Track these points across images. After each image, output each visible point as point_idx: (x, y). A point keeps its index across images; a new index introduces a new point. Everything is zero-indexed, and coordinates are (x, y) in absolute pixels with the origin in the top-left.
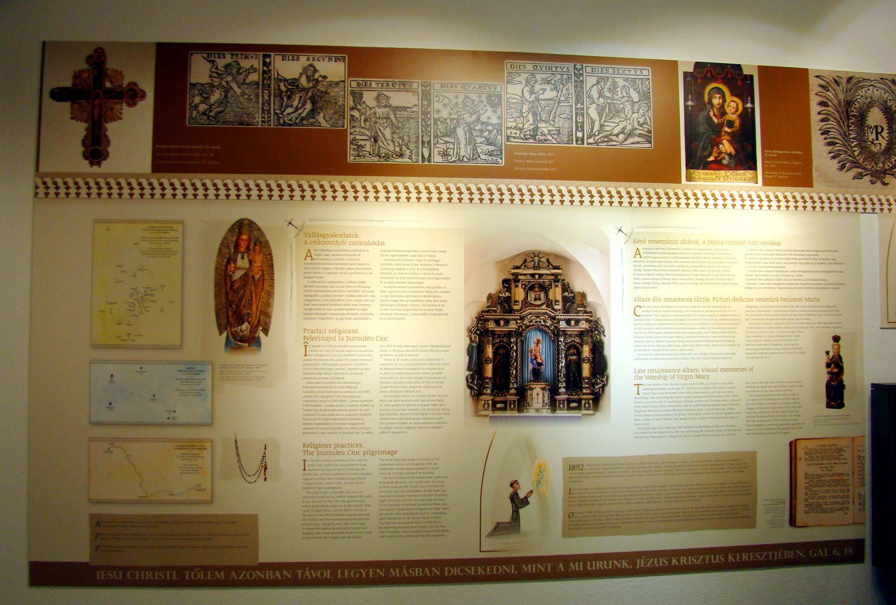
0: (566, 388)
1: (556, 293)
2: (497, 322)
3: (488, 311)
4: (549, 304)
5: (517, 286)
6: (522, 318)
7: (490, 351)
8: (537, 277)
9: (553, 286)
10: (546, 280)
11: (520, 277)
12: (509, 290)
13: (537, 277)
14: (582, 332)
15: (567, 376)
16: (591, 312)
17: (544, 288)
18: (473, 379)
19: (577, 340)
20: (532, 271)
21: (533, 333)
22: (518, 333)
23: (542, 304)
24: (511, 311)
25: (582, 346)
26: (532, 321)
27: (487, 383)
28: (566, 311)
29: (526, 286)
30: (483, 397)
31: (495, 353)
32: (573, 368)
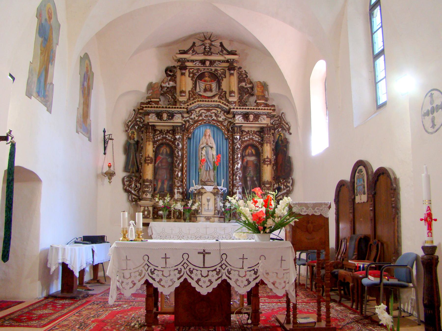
1: (231, 83)
2: (159, 115)
3: (149, 103)
4: (222, 95)
5: (183, 74)
6: (189, 112)
7: (150, 150)
8: (208, 63)
10: (219, 68)
12: (173, 78)
13: (208, 63)
14: (262, 128)
16: (273, 106)
17: (216, 78)
18: (130, 182)
19: (256, 138)
20: (201, 57)
21: (202, 129)
22: (184, 129)
23: (214, 96)
24: (175, 102)
25: (262, 145)
26: (201, 115)
27: (147, 186)
28: (242, 103)
29: (194, 74)
30: (142, 202)
31: (156, 152)
32: (251, 172)
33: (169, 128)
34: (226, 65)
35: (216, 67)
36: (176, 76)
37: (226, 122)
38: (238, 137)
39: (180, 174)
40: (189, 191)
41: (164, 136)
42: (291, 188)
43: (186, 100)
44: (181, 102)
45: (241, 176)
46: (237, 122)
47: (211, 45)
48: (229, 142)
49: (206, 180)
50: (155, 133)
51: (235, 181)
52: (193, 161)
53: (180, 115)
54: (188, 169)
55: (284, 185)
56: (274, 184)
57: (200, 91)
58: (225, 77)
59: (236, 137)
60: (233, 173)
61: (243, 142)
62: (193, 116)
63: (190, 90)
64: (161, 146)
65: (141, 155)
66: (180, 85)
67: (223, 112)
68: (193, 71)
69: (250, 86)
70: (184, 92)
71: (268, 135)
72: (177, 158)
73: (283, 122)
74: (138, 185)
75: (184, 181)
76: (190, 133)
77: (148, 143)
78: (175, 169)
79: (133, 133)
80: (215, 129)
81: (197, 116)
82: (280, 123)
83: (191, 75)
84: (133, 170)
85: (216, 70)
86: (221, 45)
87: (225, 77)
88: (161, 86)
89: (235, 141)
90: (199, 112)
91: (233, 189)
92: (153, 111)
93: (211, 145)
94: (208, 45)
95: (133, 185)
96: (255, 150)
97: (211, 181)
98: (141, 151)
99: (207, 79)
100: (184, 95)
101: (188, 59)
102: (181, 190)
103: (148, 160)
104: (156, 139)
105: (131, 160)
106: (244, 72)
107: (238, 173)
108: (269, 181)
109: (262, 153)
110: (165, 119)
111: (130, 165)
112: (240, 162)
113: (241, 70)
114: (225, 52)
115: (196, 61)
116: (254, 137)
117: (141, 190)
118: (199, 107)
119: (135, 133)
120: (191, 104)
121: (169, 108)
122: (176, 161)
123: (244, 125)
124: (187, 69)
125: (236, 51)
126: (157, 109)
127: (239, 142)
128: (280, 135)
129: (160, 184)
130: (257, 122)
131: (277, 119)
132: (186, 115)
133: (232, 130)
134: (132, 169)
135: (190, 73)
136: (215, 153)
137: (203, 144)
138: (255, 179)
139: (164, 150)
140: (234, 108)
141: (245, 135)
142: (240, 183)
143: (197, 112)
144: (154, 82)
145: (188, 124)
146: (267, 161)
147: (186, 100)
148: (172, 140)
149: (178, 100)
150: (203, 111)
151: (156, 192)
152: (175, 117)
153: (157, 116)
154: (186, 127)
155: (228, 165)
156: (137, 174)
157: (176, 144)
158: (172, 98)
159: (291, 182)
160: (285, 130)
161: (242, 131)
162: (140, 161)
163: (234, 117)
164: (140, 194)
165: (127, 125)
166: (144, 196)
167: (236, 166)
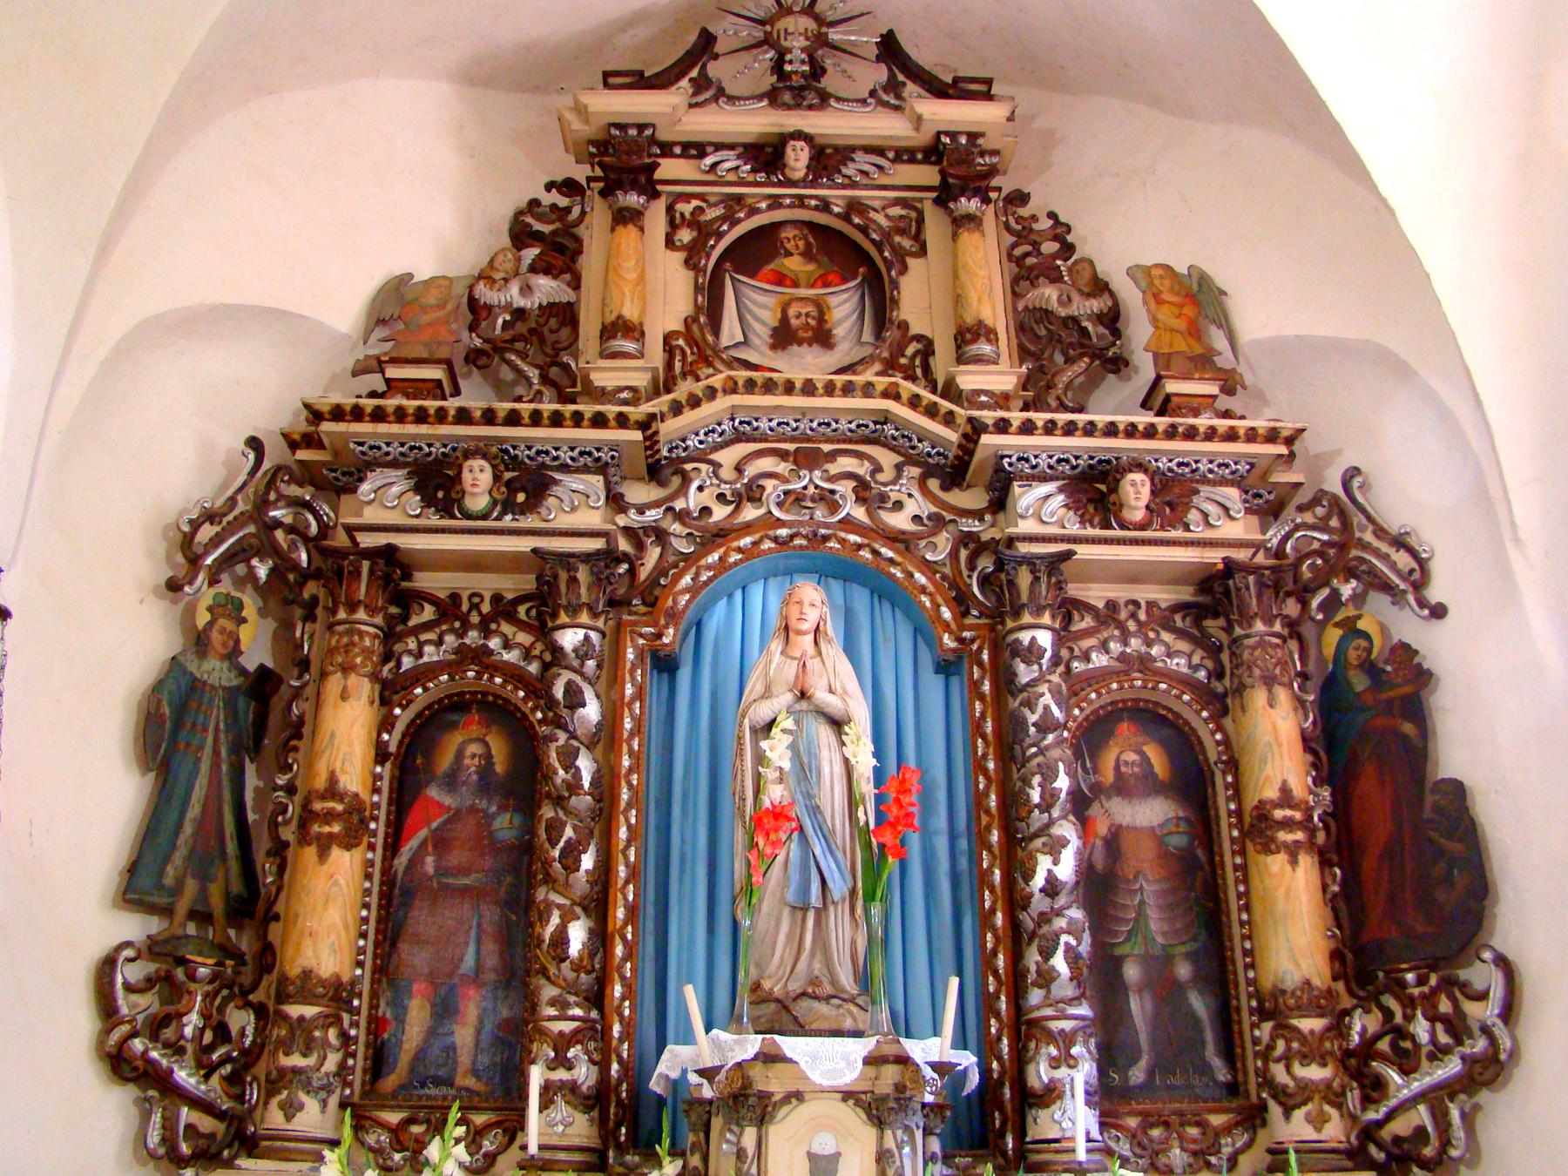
0: (1109, 1098)
2: (436, 482)
4: (907, 356)
5: (626, 217)
7: (347, 737)
8: (798, 158)
9: (935, 226)
10: (880, 194)
11: (670, 168)
13: (798, 158)
15: (1102, 975)
19: (1176, 656)
20: (755, 122)
21: (763, 598)
22: (623, 584)
26: (752, 493)
31: (407, 765)
33: (511, 585)
34: (928, 175)
35: (854, 185)
36: (578, 241)
37: (944, 541)
38: (1045, 639)
39: (578, 935)
40: (656, 1085)
41: (473, 638)
42: (1505, 1043)
43: (641, 380)
44: (603, 395)
45: (1084, 948)
46: (1027, 526)
47: (821, 41)
48: (975, 686)
49: (795, 986)
50: (405, 618)
51: (1035, 996)
52: (690, 834)
53: (597, 481)
54: (651, 895)
55: (1433, 1018)
56: (1347, 1013)
57: (746, 343)
58: (922, 251)
59: (1025, 637)
60: (1014, 925)
61: (1075, 688)
62: (693, 500)
63: (677, 326)
64: (455, 717)
65: (281, 780)
66: (606, 283)
67: (915, 471)
68: (700, 210)
69: (1095, 305)
70: (633, 331)
71: (1269, 621)
72: (559, 801)
73: (1368, 537)
74: (241, 1020)
75: (618, 990)
76: (673, 616)
77: (335, 683)
78: (541, 894)
79: (230, 609)
80: (861, 599)
81: (721, 497)
82: (1345, 540)
83: (685, 236)
84: (203, 893)
85: (855, 207)
86: (890, 49)
88: (473, 303)
89: (1025, 673)
90: (739, 469)
91: (1021, 1059)
92: (396, 450)
93: (833, 703)
94: (797, 44)
95: (193, 1021)
96: (1165, 745)
97: (836, 996)
98: (287, 748)
99: (794, 264)
100: (629, 346)
101: (664, 135)
102: (584, 1073)
103: (329, 817)
104: (407, 662)
105: (194, 810)
106: (1045, 224)
107: (1061, 923)
108: (1316, 982)
109: (1233, 765)
110: (478, 501)
111: (179, 857)
112: (1067, 830)
113: (1024, 212)
114: (911, 88)
115: (719, 147)
116: (1155, 651)
117: (260, 1069)
118: (739, 438)
119: (250, 611)
120: (677, 409)
121: (513, 419)
122: (554, 829)
123: (1083, 551)
124: (655, 195)
125: (989, 82)
126: (424, 429)
127: (1055, 678)
128: (1351, 629)
129: (418, 1015)
130: (1178, 533)
131: (1308, 518)
132: (637, 493)
133: (996, 588)
134: (191, 886)
135: (673, 226)
136: (865, 762)
137: (767, 694)
138: (1183, 971)
139: (471, 747)
140: (1002, 427)
141: (1087, 633)
142: (1084, 1010)
143: (727, 473)
144: (423, 273)
145: (653, 554)
146: (1288, 824)
147: (641, 380)
148: (534, 668)
149: (587, 381)
150: (767, 464)
151: (390, 1082)
152: (556, 490)
153: (417, 489)
155: (963, 863)
156: (245, 942)
157: (559, 692)
158: (545, 379)
159: (1497, 993)
160: (1386, 587)
161: (1068, 609)
162: (274, 826)
163: (999, 503)
164: (253, 1094)
165: (187, 541)
166: (275, 1118)
167: (1044, 863)
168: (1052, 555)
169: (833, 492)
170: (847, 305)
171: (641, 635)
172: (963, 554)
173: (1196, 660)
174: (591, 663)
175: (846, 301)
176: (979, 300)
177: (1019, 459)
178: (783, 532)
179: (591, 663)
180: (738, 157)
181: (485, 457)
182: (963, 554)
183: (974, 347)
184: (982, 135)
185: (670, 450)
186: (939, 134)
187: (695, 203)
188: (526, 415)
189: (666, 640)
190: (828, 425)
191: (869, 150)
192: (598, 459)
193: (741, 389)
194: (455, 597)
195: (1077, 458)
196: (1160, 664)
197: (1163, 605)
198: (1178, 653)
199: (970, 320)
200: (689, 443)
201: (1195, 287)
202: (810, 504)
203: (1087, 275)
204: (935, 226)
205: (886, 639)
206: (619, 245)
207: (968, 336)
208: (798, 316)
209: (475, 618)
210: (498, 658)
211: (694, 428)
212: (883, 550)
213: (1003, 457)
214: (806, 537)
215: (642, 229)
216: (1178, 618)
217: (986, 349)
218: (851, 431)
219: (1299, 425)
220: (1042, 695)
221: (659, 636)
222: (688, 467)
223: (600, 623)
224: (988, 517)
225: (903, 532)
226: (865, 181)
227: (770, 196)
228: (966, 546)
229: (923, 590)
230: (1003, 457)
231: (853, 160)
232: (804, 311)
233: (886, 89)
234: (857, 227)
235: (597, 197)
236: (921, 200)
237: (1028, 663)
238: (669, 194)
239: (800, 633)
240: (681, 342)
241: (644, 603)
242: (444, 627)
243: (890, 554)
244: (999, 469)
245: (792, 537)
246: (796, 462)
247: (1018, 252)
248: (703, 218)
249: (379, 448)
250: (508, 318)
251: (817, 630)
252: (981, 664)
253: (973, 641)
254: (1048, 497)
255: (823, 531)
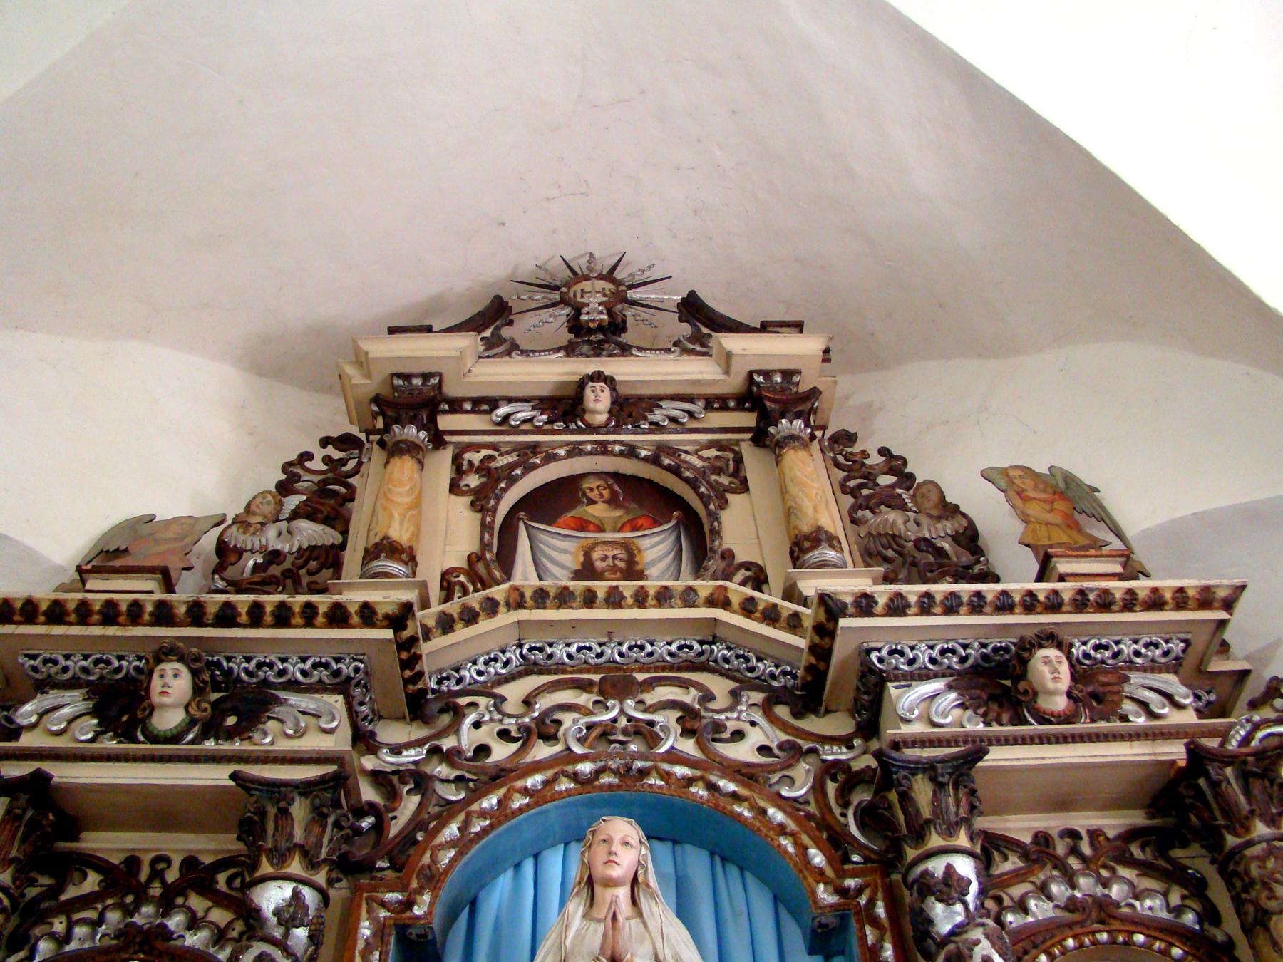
8: (599, 402)
9: (754, 462)
20: (552, 371)
26: (546, 729)
38: (965, 867)
53: (337, 701)
58: (744, 487)
59: (937, 867)
62: (468, 738)
67: (757, 697)
68: (491, 458)
69: (948, 526)
76: (432, 879)
80: (697, 862)
81: (504, 735)
83: (473, 481)
86: (692, 308)
87: (744, 487)
89: (945, 917)
90: (528, 702)
100: (396, 567)
101: (451, 390)
106: (875, 459)
110: (169, 719)
118: (530, 668)
135: (459, 470)
140: (865, 605)
141: (1016, 877)
145: (410, 804)
152: (279, 710)
154: (394, 829)
168: (955, 757)
169: (651, 723)
170: (661, 546)
171: (383, 904)
172: (831, 788)
173: (1175, 899)
174: (301, 933)
175: (658, 543)
176: (815, 509)
177: (891, 653)
178: (586, 768)
179: (301, 933)
180: (533, 408)
181: (181, 659)
182: (831, 788)
183: (816, 552)
184: (799, 372)
185: (440, 682)
186: (751, 373)
187: (485, 452)
188: (243, 610)
189: (417, 911)
190: (642, 648)
191: (673, 398)
192: (337, 673)
193: (530, 602)
194: (133, 862)
195: (965, 647)
196: (1126, 910)
197: (1111, 834)
198: (1149, 893)
199: (806, 528)
200: (465, 673)
201: (1062, 485)
202: (621, 738)
203: (934, 497)
204: (754, 462)
205: (734, 915)
206: (392, 473)
207: (807, 544)
208: (604, 558)
209: (156, 890)
210: (179, 943)
211: (470, 652)
212: (722, 783)
213: (869, 651)
214: (615, 772)
215: (421, 463)
216: (1136, 850)
217: (831, 554)
218: (671, 654)
219: (1237, 582)
220: (977, 942)
221: (409, 904)
222: (463, 701)
223: (321, 878)
224: (857, 742)
225: (748, 765)
226: (673, 426)
227: (568, 443)
228: (834, 779)
229: (782, 830)
230: (869, 651)
231: (660, 407)
232: (611, 554)
233: (690, 340)
234: (668, 468)
235: (376, 446)
236: (737, 442)
237: (947, 901)
238: (457, 444)
239: (610, 883)
240: (462, 578)
241: (393, 867)
242: (110, 902)
243: (731, 787)
244: (867, 670)
245: (598, 773)
246: (601, 693)
247: (852, 483)
248: (493, 465)
249: (55, 662)
250: (260, 561)
251: (635, 881)
252: (875, 922)
253: (860, 891)
254: (934, 697)
255: (638, 764)
